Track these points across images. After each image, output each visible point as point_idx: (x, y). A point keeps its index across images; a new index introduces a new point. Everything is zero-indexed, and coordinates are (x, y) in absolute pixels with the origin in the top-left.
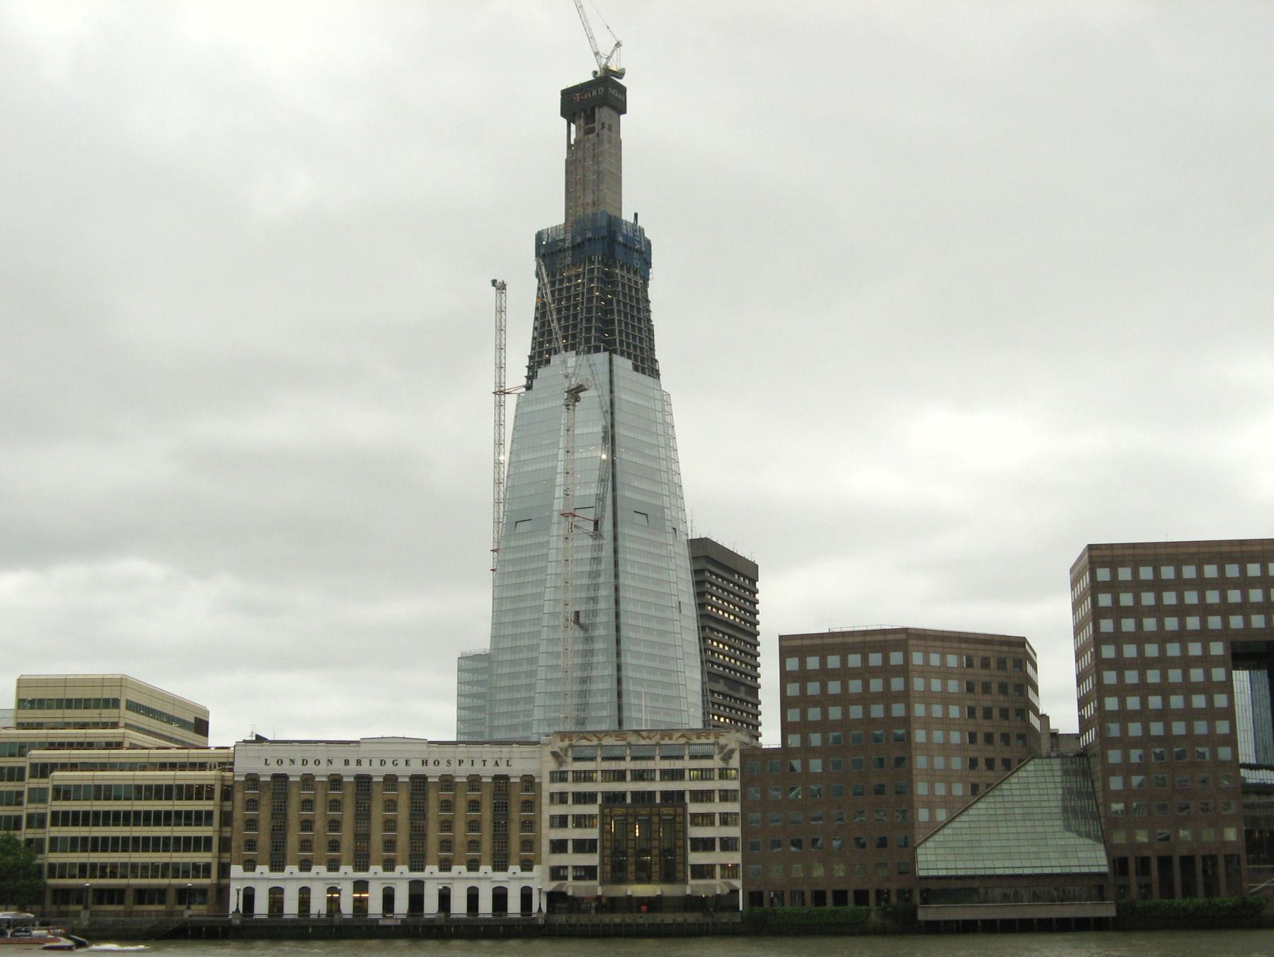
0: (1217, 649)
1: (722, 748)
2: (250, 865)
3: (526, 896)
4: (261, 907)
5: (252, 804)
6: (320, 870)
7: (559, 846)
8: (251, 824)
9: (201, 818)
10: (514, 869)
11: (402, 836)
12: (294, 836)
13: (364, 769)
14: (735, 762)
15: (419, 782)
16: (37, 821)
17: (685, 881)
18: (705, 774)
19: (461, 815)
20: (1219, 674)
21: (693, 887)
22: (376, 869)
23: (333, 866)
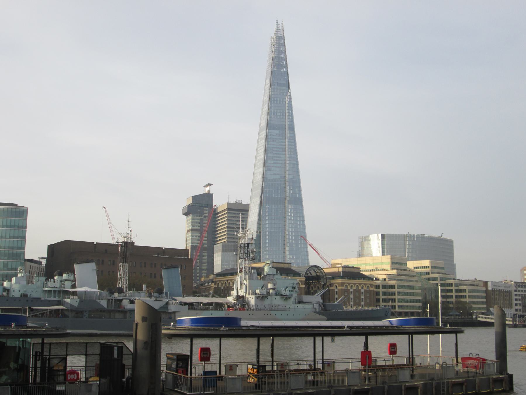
7: (516, 305)
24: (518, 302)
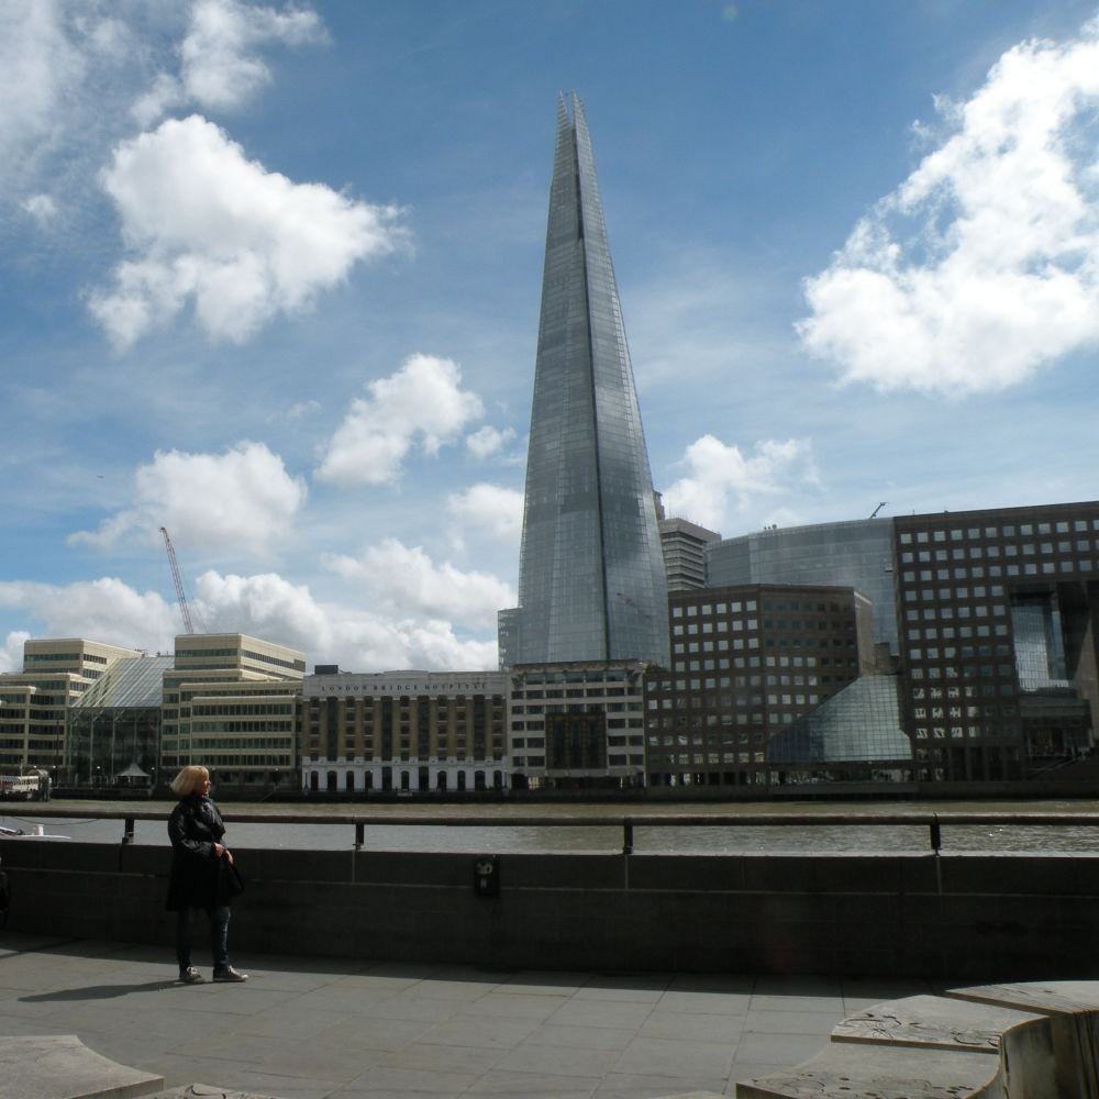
0: (997, 590)
1: (629, 673)
2: (314, 757)
3: (497, 776)
4: (323, 784)
5: (315, 717)
6: (359, 760)
7: (518, 743)
8: (315, 730)
9: (284, 726)
10: (489, 759)
11: (413, 737)
12: (342, 738)
13: (387, 693)
14: (639, 683)
15: (423, 700)
16: (185, 729)
17: (605, 767)
18: (620, 692)
19: (452, 722)
20: (999, 610)
21: (610, 770)
22: (396, 760)
23: (368, 757)
24: (526, 734)
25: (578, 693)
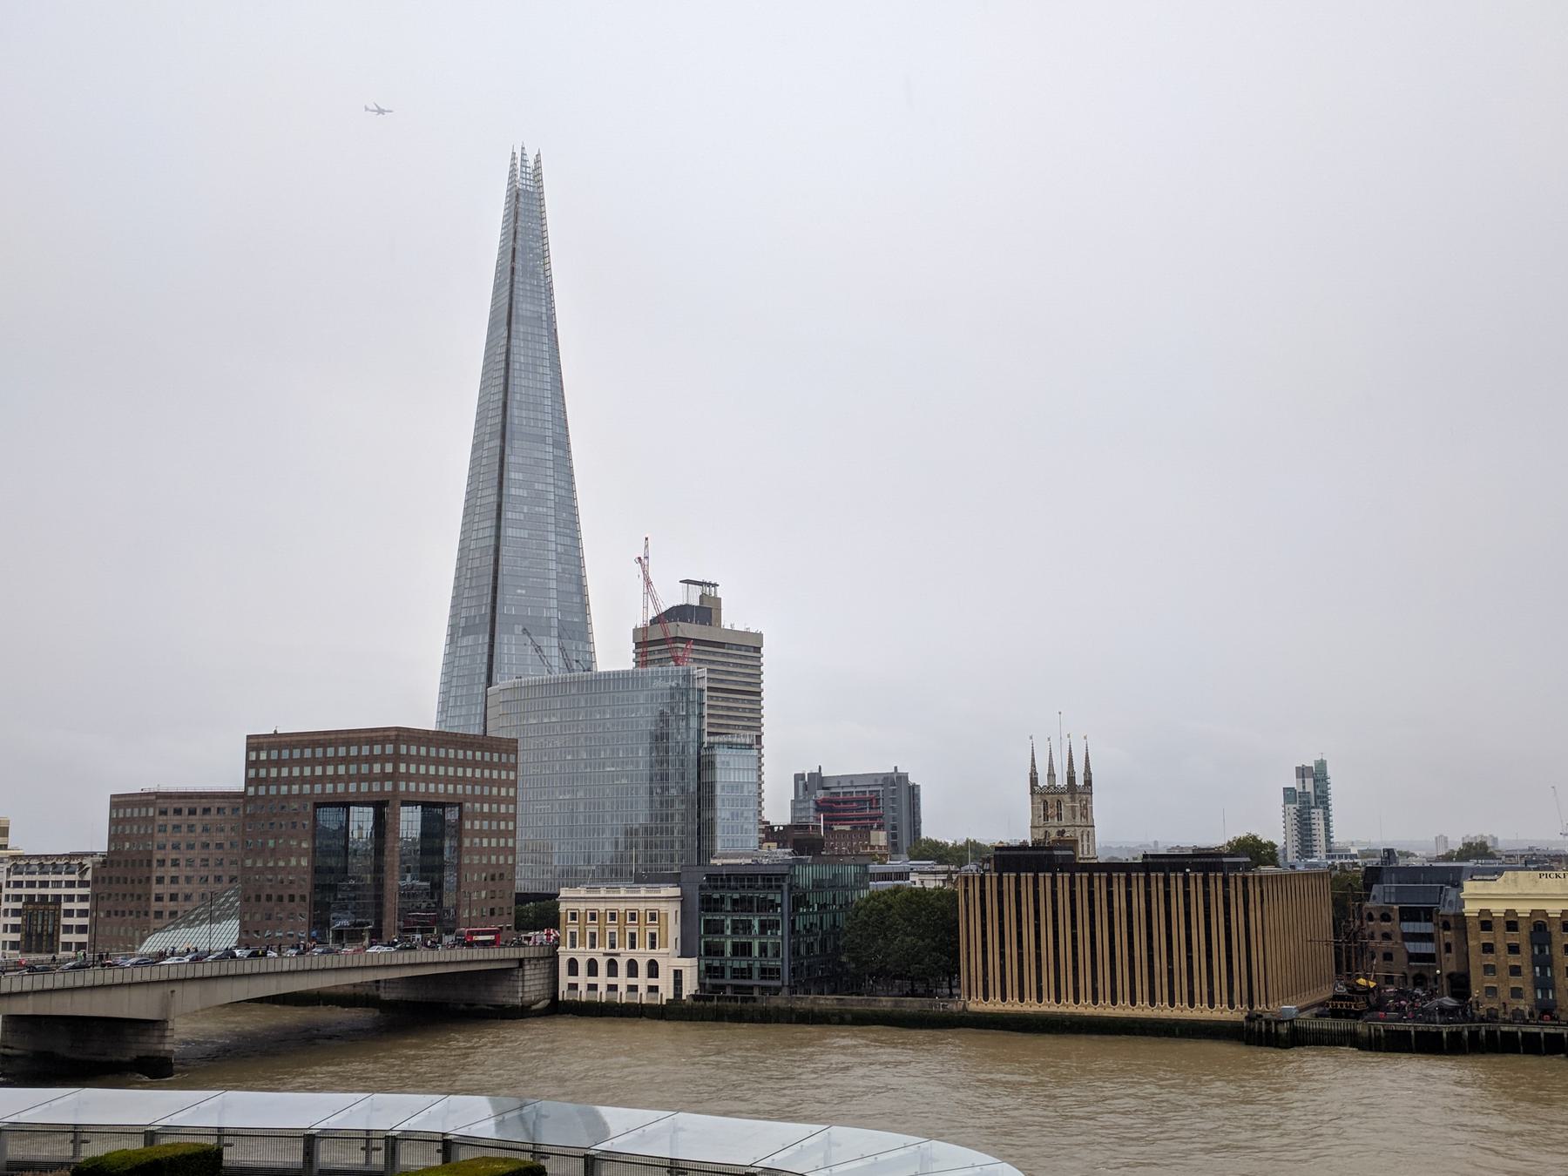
18: (70, 884)
25: (44, 884)
